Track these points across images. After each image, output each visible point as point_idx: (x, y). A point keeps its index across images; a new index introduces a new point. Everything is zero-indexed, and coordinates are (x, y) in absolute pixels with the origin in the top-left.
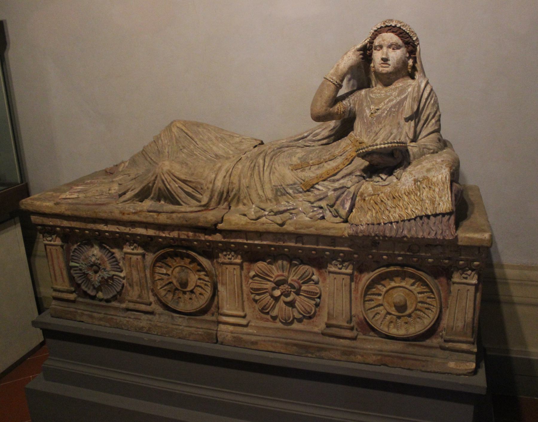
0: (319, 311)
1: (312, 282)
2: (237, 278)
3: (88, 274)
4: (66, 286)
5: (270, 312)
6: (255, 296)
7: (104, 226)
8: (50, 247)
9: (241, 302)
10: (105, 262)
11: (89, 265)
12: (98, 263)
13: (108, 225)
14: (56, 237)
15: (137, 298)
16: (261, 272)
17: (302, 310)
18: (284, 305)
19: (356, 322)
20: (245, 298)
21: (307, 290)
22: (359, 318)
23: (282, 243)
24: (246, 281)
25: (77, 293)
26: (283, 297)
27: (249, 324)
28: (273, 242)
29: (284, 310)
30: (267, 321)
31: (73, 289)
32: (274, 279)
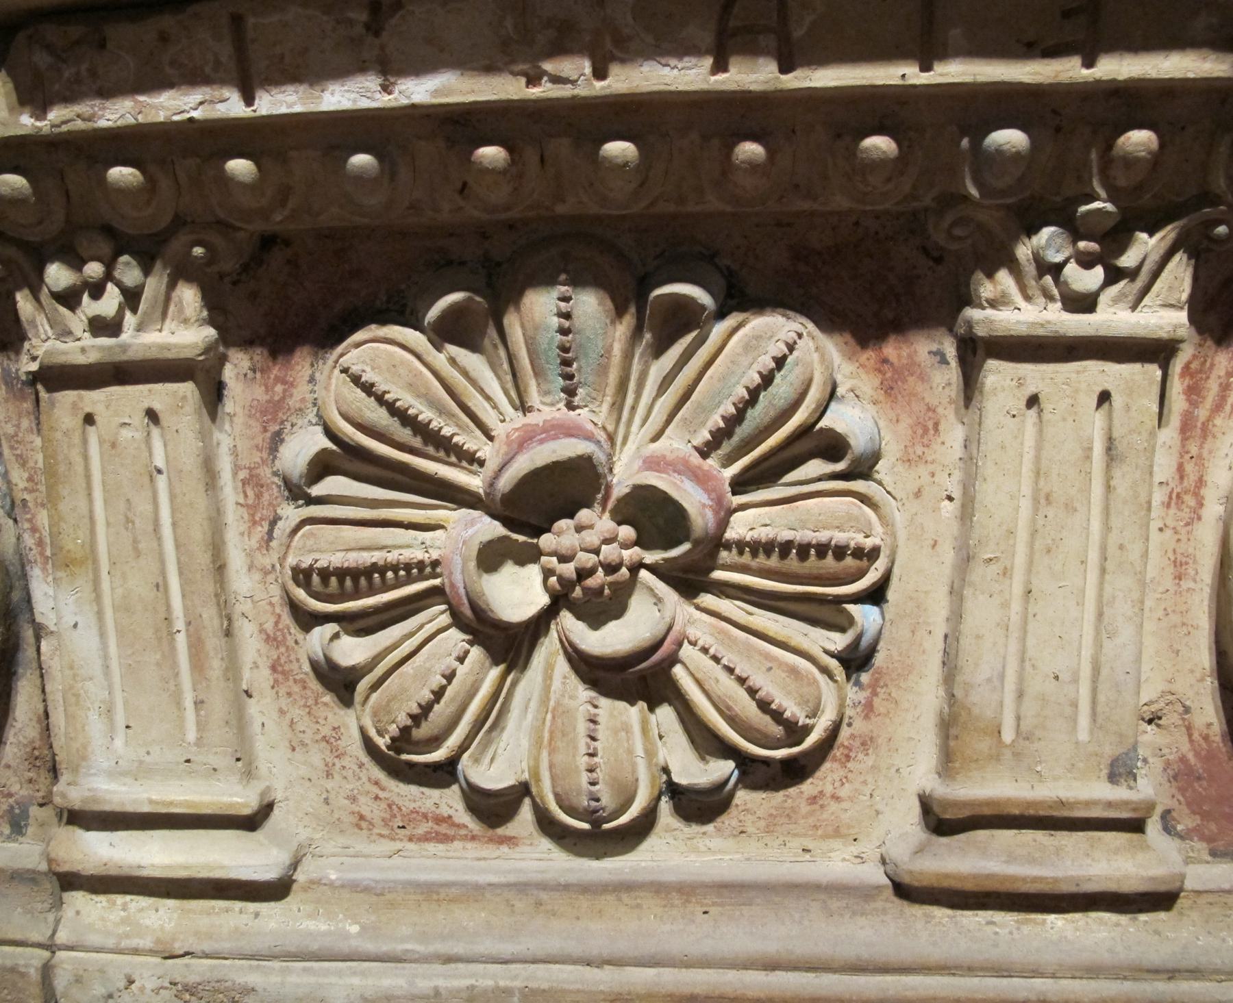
0: (869, 708)
1: (815, 467)
2: (172, 497)
5: (465, 763)
6: (336, 636)
9: (218, 705)
16: (380, 417)
17: (732, 720)
18: (584, 693)
19: (1168, 764)
20: (256, 674)
21: (785, 535)
22: (1189, 729)
23: (587, 67)
24: (255, 523)
26: (567, 619)
27: (300, 876)
28: (490, 69)
29: (582, 727)
30: (445, 839)
32: (491, 465)
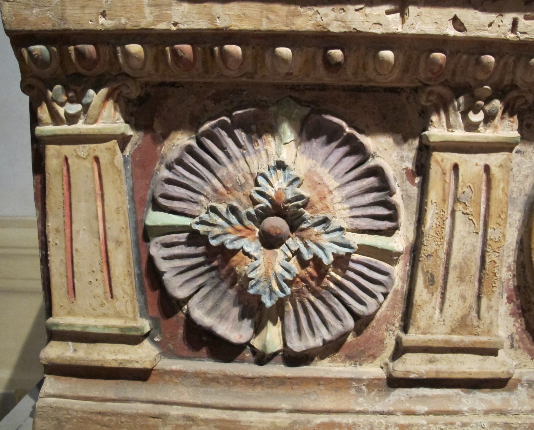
3: (235, 252)
4: (119, 315)
7: (388, 13)
8: (67, 149)
10: (330, 192)
11: (252, 210)
12: (300, 197)
13: (412, 10)
14: (108, 97)
15: (453, 331)
25: (157, 339)
31: (146, 325)
